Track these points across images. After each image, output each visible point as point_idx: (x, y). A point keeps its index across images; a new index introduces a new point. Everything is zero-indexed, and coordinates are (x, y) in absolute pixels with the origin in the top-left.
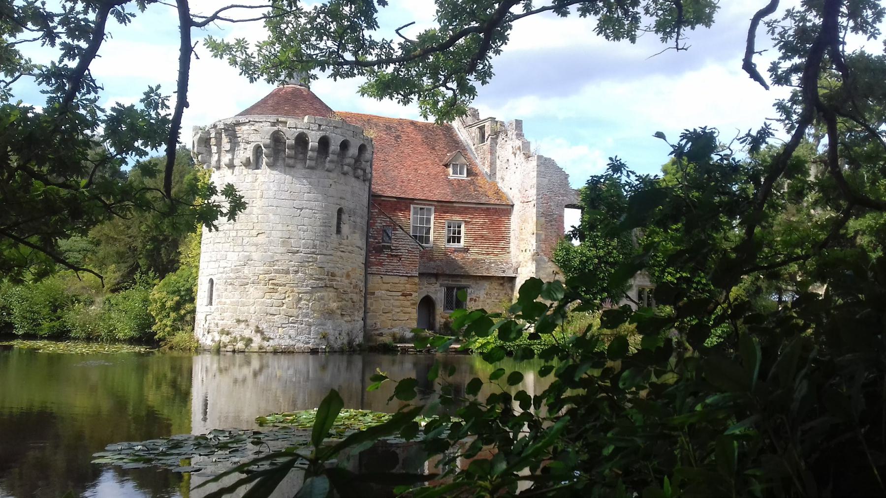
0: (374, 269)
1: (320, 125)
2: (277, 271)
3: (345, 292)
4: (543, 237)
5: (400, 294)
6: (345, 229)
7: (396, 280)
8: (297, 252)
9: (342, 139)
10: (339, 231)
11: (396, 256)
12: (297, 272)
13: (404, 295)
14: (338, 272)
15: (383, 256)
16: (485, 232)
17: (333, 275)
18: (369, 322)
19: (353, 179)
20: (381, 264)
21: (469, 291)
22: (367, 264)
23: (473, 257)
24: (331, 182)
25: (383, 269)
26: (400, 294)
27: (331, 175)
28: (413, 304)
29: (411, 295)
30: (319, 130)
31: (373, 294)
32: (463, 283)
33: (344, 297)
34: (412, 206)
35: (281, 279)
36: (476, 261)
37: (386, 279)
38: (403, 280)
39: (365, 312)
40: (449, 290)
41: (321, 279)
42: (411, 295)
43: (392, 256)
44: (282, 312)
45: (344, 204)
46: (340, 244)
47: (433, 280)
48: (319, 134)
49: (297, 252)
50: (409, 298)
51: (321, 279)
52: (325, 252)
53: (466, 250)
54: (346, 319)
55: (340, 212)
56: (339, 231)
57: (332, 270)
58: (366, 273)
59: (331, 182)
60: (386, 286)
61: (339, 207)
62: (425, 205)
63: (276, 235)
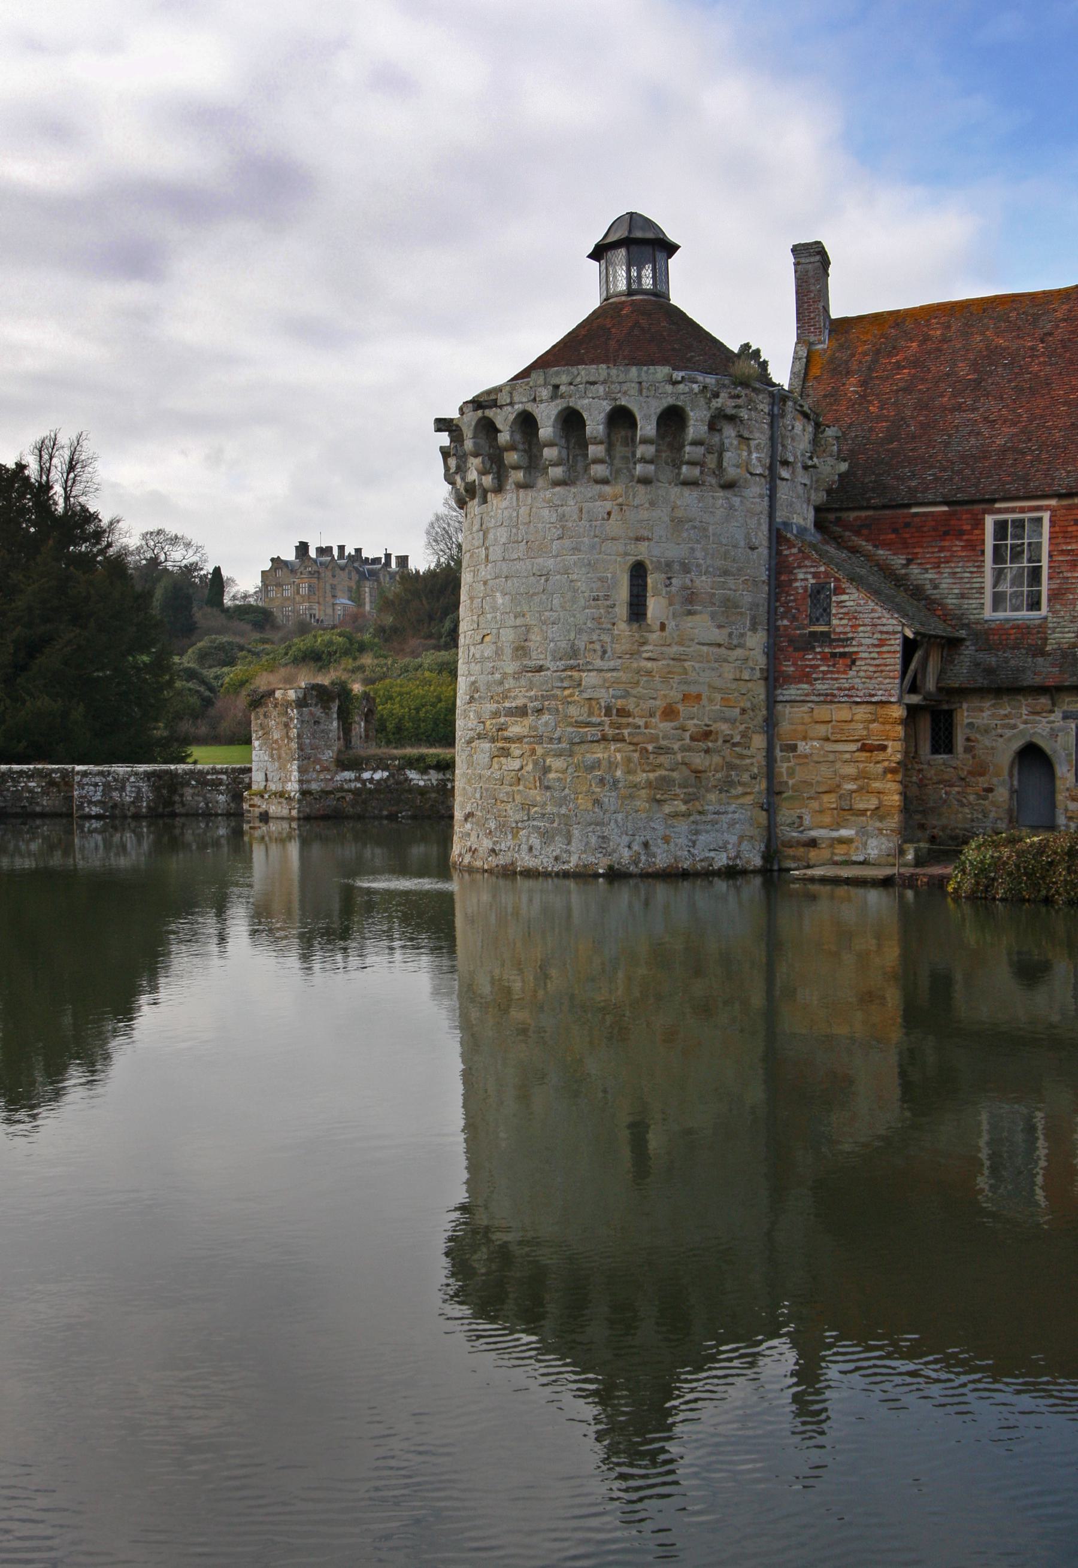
0: (792, 692)
1: (556, 387)
3: (660, 750)
5: (859, 744)
6: (655, 607)
7: (844, 713)
8: (540, 669)
9: (607, 406)
10: (637, 610)
11: (843, 655)
12: (539, 711)
13: (864, 748)
14: (630, 704)
17: (623, 712)
18: (786, 814)
20: (805, 677)
22: (773, 679)
24: (608, 505)
27: (607, 489)
28: (893, 771)
29: (884, 748)
31: (794, 748)
33: (662, 759)
34: (989, 521)
35: (516, 729)
37: (823, 712)
38: (862, 712)
39: (774, 792)
41: (588, 724)
42: (884, 748)
43: (833, 655)
44: (518, 798)
45: (642, 552)
46: (644, 644)
47: (1044, 701)
49: (540, 669)
50: (881, 756)
51: (588, 724)
52: (598, 663)
54: (667, 809)
55: (638, 572)
56: (637, 610)
57: (620, 703)
58: (772, 702)
59: (608, 505)
60: (822, 730)
61: (631, 559)
62: (1022, 510)
63: (508, 636)
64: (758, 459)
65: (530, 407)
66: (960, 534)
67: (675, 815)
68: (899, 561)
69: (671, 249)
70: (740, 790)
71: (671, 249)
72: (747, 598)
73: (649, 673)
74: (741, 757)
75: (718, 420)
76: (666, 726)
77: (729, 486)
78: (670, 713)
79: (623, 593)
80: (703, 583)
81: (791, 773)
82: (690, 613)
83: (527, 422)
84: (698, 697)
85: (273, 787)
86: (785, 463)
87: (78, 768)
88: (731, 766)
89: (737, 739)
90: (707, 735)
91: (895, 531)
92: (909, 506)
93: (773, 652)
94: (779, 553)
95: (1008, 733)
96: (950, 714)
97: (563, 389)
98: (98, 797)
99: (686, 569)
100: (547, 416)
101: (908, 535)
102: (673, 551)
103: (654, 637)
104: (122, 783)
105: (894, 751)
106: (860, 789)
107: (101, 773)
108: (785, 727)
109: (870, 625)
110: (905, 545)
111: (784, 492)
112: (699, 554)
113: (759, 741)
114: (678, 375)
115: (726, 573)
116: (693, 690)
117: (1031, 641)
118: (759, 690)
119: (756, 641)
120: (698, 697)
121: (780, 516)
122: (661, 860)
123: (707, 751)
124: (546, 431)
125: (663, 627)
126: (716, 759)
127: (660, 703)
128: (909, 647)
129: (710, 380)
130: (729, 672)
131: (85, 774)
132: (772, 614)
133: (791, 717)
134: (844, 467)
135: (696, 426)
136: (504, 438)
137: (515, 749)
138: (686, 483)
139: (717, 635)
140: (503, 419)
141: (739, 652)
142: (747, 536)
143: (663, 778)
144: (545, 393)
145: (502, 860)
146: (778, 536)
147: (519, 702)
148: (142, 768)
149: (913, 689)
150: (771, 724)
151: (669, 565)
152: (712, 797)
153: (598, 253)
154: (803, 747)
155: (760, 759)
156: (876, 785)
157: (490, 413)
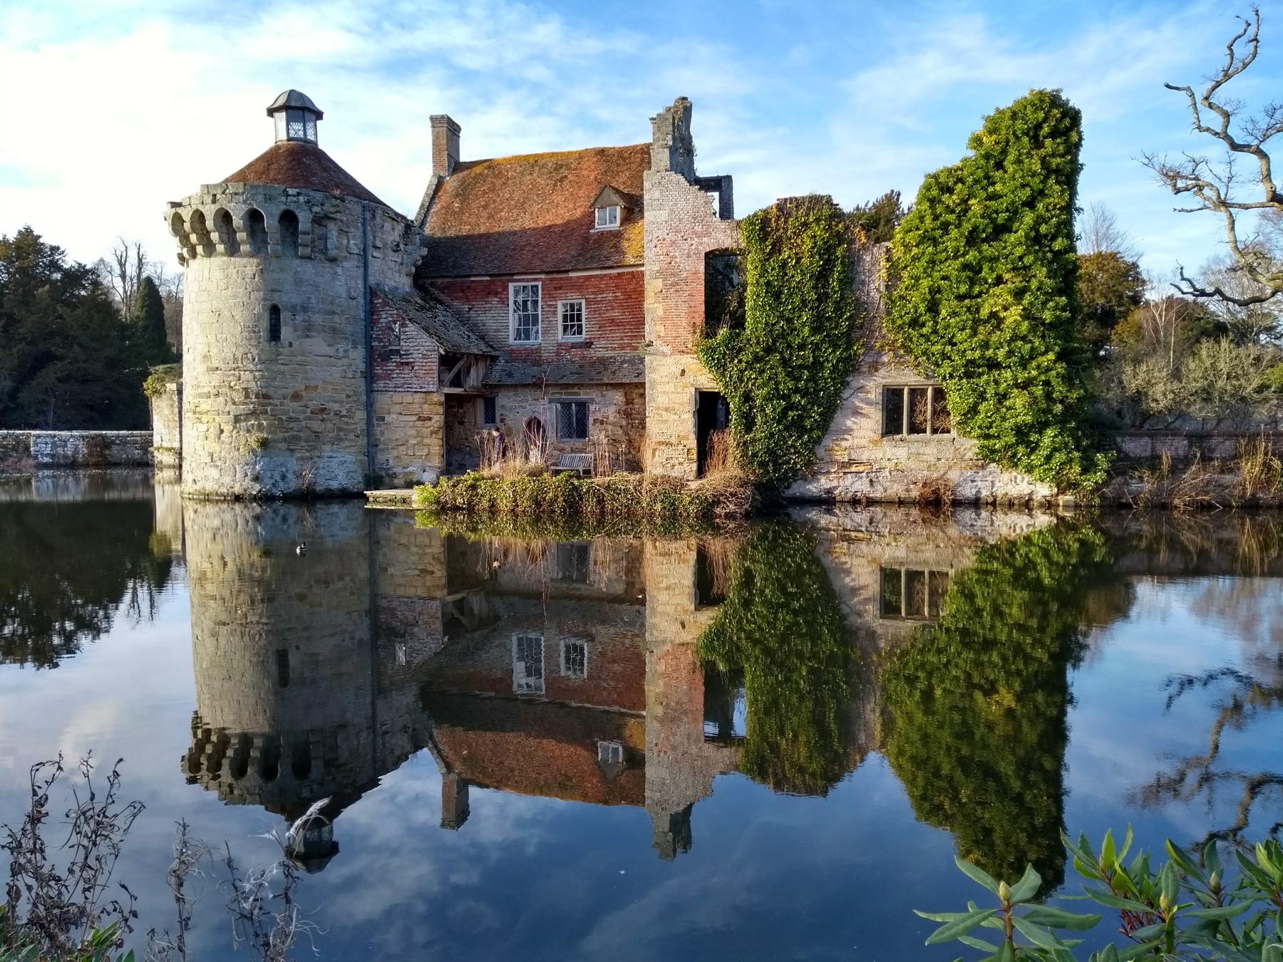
1: (215, 196)
2: (200, 395)
4: (660, 312)
5: (414, 418)
6: (286, 332)
7: (408, 398)
9: (245, 208)
10: (274, 334)
11: (407, 364)
13: (420, 419)
15: (391, 365)
16: (616, 314)
18: (381, 457)
19: (298, 261)
20: (389, 377)
21: (592, 408)
22: (370, 377)
23: (599, 355)
25: (391, 384)
26: (414, 418)
28: (436, 432)
30: (214, 201)
31: (383, 419)
32: (583, 395)
34: (511, 286)
36: (603, 361)
37: (397, 398)
38: (418, 398)
40: (566, 405)
42: (430, 419)
43: (402, 364)
48: (217, 206)
50: (428, 423)
53: (588, 345)
55: (275, 311)
58: (370, 391)
60: (397, 408)
62: (528, 280)
64: (355, 244)
65: (201, 208)
66: (496, 294)
67: (302, 458)
68: (466, 307)
69: (319, 115)
70: (347, 443)
71: (319, 115)
72: (349, 328)
73: (283, 373)
74: (348, 424)
75: (319, 220)
76: (295, 404)
77: (333, 260)
78: (296, 397)
79: (265, 324)
80: (317, 319)
81: (382, 433)
82: (308, 336)
83: (224, 217)
84: (316, 387)
85: (165, 445)
86: (376, 247)
87: (33, 432)
88: (340, 429)
89: (344, 413)
90: (323, 410)
91: (462, 291)
92: (469, 276)
93: (370, 360)
94: (371, 302)
95: (521, 410)
96: (493, 399)
97: (218, 196)
98: (48, 451)
99: (305, 309)
100: (209, 211)
101: (468, 292)
102: (296, 299)
103: (286, 350)
104: (65, 443)
105: (438, 420)
106: (419, 443)
107: (47, 436)
108: (378, 406)
109: (421, 347)
110: (468, 300)
111: (375, 266)
112: (313, 301)
113: (360, 415)
114: (291, 191)
115: (333, 313)
116: (313, 383)
117: (533, 358)
118: (361, 385)
119: (358, 355)
120: (316, 387)
121: (372, 281)
122: (292, 485)
123: (323, 420)
124: (210, 224)
125: (291, 345)
126: (329, 425)
127: (291, 391)
128: (447, 361)
129: (319, 196)
130: (336, 373)
131: (38, 437)
132: (368, 339)
133: (382, 401)
134: (424, 251)
135: (304, 220)
136: (187, 226)
137: (204, 419)
138: (302, 257)
139: (330, 351)
140: (186, 214)
141: (345, 361)
142: (348, 291)
143: (294, 437)
144: (209, 199)
145: (198, 487)
146: (371, 293)
147: (206, 390)
148: (75, 433)
149: (456, 382)
150: (369, 406)
151: (294, 307)
152: (327, 447)
153: (271, 112)
154: (388, 419)
155: (362, 425)
156: (427, 441)
157: (180, 210)
